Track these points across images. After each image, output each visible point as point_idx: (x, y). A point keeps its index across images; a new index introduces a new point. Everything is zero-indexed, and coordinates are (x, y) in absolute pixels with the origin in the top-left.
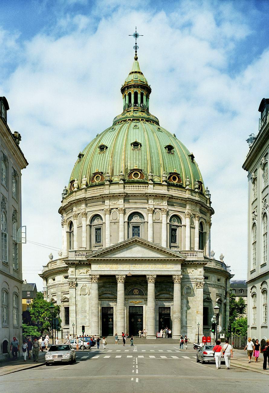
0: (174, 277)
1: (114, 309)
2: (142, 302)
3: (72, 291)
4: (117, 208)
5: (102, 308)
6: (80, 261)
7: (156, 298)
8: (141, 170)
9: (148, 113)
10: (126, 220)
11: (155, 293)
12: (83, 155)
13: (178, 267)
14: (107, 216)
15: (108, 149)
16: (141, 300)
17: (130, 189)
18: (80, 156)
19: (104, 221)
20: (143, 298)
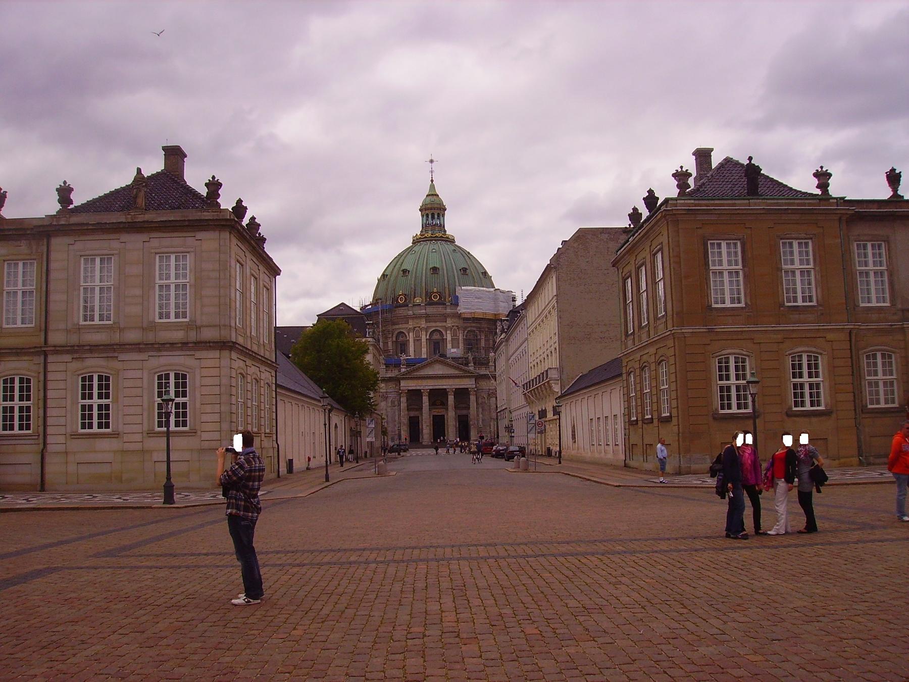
0: (470, 390)
1: (420, 417)
2: (443, 411)
3: (383, 404)
4: (419, 327)
5: (409, 417)
6: (390, 377)
7: (455, 407)
8: (440, 293)
9: (445, 231)
10: (428, 337)
11: (455, 403)
12: (387, 275)
13: (473, 381)
14: (411, 334)
15: (410, 272)
16: (442, 410)
17: (431, 310)
18: (384, 276)
19: (408, 338)
20: (444, 408)
